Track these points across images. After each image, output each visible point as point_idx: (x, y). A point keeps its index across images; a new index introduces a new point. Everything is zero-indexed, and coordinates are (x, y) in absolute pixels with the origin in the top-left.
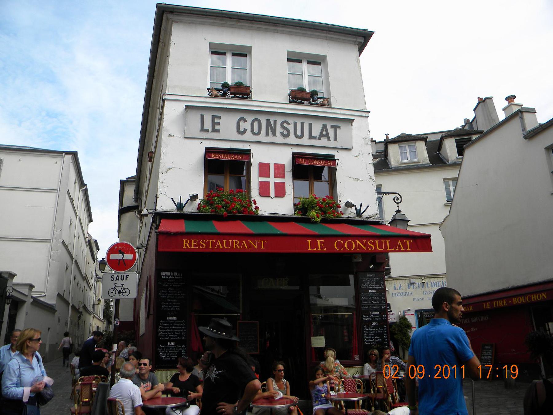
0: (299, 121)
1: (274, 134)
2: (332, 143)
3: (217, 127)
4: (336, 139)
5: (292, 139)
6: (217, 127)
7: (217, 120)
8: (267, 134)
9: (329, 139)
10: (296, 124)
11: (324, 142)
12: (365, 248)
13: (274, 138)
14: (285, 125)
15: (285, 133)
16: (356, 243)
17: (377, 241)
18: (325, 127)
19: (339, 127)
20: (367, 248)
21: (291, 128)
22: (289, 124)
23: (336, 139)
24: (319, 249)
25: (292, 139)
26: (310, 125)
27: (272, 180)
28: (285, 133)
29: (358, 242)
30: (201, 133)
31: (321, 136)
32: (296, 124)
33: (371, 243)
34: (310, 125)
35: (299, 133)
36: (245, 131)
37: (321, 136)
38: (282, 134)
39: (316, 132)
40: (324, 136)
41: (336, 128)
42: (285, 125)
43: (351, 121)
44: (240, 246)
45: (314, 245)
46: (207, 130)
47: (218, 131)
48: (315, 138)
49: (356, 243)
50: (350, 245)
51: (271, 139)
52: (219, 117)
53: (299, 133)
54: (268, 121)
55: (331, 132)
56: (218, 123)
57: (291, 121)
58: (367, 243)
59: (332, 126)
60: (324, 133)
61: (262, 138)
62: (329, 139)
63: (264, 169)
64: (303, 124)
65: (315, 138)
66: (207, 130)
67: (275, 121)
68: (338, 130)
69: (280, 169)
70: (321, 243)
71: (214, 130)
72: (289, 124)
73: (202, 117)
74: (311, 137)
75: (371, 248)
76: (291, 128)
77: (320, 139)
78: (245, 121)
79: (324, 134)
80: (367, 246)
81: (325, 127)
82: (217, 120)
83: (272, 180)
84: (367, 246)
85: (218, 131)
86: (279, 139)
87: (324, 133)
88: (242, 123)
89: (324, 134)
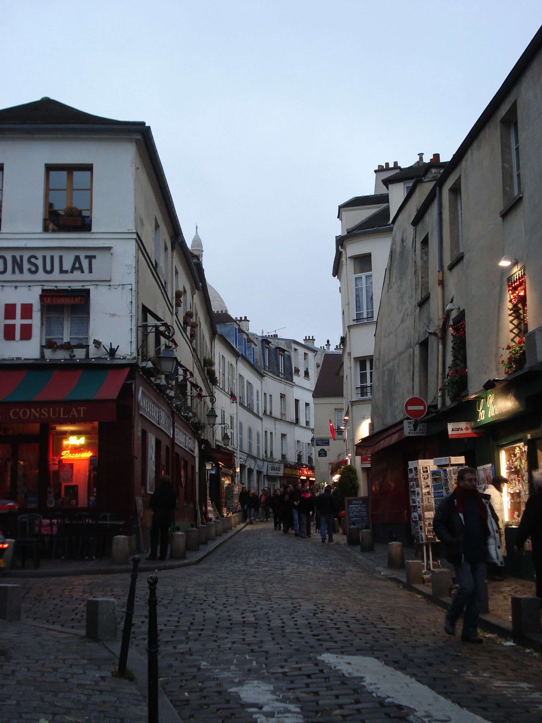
0: (48, 254)
1: (21, 271)
2: (86, 276)
4: (91, 271)
5: (41, 275)
8: (14, 272)
9: (82, 272)
10: (44, 258)
11: (77, 275)
12: (38, 416)
13: (21, 275)
14: (33, 260)
15: (33, 269)
18: (77, 258)
19: (94, 257)
20: (40, 416)
21: (40, 263)
22: (36, 258)
23: (91, 271)
25: (41, 275)
26: (61, 258)
27: (18, 322)
28: (33, 269)
29: (33, 410)
31: (73, 269)
32: (44, 258)
33: (45, 410)
34: (61, 258)
35: (48, 268)
37: (73, 269)
38: (30, 270)
39: (67, 266)
40: (78, 269)
41: (90, 258)
42: (33, 260)
43: (109, 248)
48: (66, 272)
50: (25, 413)
51: (18, 276)
53: (48, 268)
54: (14, 258)
55: (85, 263)
57: (40, 255)
58: (41, 410)
59: (86, 257)
60: (77, 265)
62: (82, 272)
64: (52, 258)
65: (66, 272)
67: (21, 257)
68: (94, 261)
69: (27, 310)
72: (36, 258)
74: (62, 271)
75: (44, 415)
76: (40, 263)
77: (72, 272)
79: (77, 266)
81: (77, 258)
83: (18, 322)
84: (41, 413)
86: (27, 276)
87: (77, 265)
89: (77, 266)
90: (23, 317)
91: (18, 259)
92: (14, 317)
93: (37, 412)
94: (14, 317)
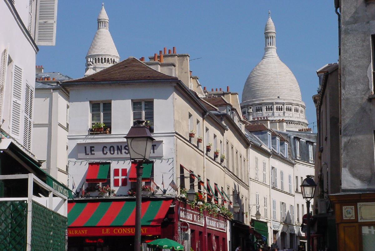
1: (121, 153)
3: (93, 153)
6: (93, 153)
7: (92, 149)
12: (126, 232)
16: (123, 230)
17: (132, 229)
20: (127, 233)
24: (107, 233)
29: (123, 229)
30: (86, 156)
36: (107, 153)
44: (78, 233)
45: (105, 231)
46: (89, 154)
47: (94, 154)
49: (123, 230)
52: (93, 147)
56: (93, 150)
58: (127, 229)
61: (116, 155)
63: (116, 172)
66: (89, 154)
67: (121, 146)
68: (155, 147)
70: (108, 230)
71: (92, 154)
73: (85, 147)
78: (106, 148)
80: (127, 231)
82: (92, 149)
84: (127, 231)
85: (94, 154)
86: (124, 155)
88: (105, 148)
90: (122, 175)
91: (120, 147)
92: (118, 175)
93: (125, 230)
94: (118, 175)
